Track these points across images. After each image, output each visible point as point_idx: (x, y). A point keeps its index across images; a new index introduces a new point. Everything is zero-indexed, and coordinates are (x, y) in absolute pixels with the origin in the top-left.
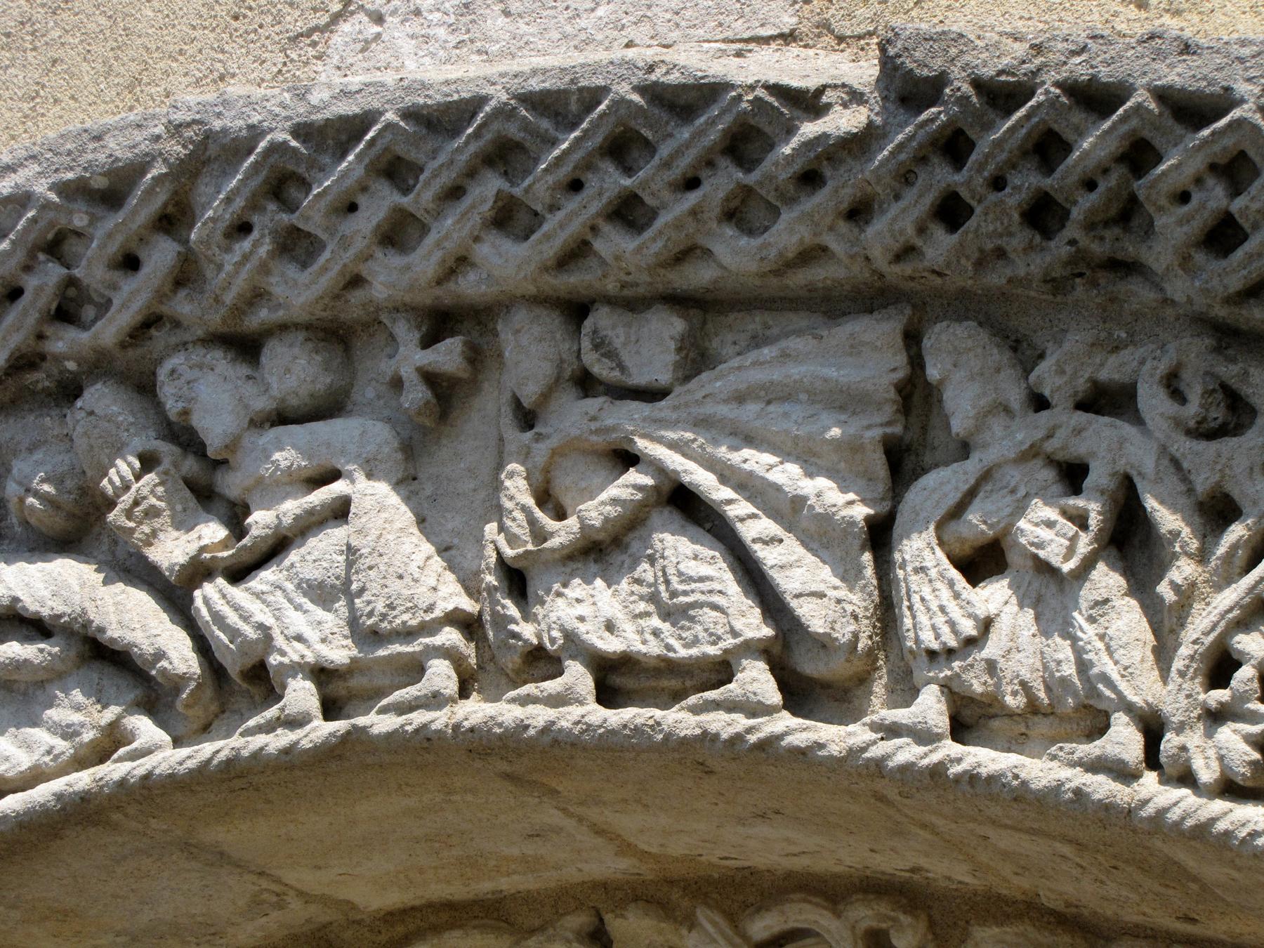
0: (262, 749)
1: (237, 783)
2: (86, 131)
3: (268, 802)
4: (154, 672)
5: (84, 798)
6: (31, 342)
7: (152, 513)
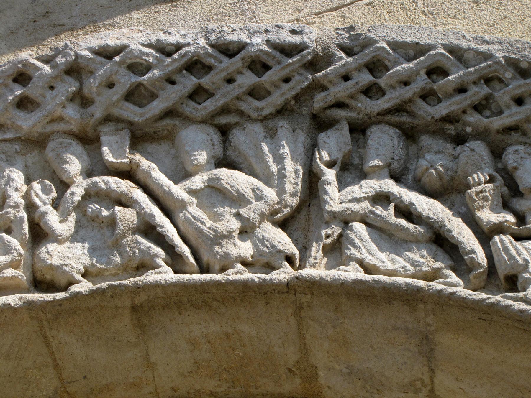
0: (511, 305)
1: (485, 316)
2: (528, 43)
3: (486, 332)
4: (466, 257)
5: (419, 290)
6: (460, 112)
7: (485, 199)
